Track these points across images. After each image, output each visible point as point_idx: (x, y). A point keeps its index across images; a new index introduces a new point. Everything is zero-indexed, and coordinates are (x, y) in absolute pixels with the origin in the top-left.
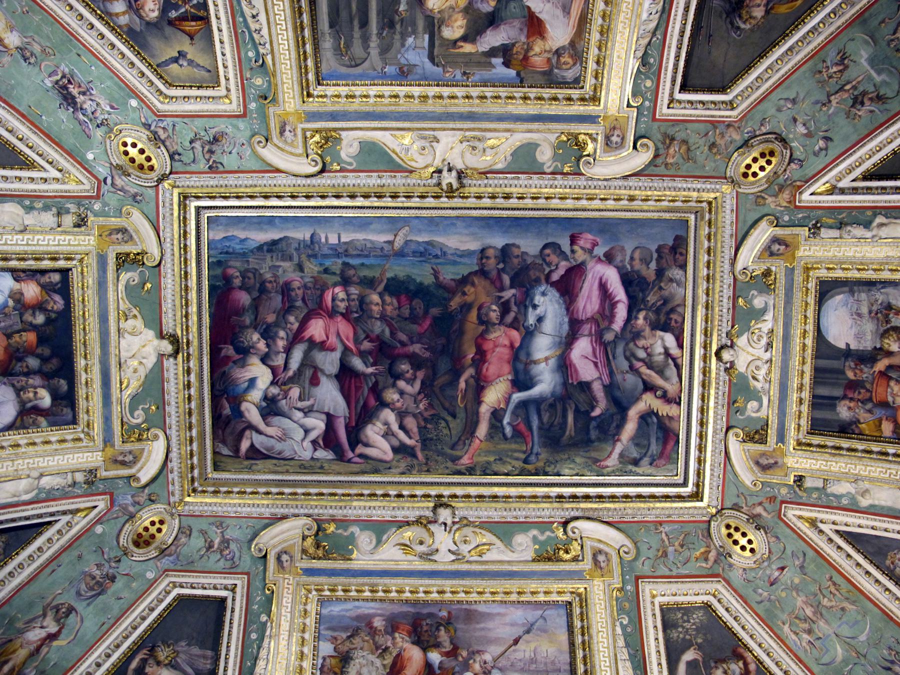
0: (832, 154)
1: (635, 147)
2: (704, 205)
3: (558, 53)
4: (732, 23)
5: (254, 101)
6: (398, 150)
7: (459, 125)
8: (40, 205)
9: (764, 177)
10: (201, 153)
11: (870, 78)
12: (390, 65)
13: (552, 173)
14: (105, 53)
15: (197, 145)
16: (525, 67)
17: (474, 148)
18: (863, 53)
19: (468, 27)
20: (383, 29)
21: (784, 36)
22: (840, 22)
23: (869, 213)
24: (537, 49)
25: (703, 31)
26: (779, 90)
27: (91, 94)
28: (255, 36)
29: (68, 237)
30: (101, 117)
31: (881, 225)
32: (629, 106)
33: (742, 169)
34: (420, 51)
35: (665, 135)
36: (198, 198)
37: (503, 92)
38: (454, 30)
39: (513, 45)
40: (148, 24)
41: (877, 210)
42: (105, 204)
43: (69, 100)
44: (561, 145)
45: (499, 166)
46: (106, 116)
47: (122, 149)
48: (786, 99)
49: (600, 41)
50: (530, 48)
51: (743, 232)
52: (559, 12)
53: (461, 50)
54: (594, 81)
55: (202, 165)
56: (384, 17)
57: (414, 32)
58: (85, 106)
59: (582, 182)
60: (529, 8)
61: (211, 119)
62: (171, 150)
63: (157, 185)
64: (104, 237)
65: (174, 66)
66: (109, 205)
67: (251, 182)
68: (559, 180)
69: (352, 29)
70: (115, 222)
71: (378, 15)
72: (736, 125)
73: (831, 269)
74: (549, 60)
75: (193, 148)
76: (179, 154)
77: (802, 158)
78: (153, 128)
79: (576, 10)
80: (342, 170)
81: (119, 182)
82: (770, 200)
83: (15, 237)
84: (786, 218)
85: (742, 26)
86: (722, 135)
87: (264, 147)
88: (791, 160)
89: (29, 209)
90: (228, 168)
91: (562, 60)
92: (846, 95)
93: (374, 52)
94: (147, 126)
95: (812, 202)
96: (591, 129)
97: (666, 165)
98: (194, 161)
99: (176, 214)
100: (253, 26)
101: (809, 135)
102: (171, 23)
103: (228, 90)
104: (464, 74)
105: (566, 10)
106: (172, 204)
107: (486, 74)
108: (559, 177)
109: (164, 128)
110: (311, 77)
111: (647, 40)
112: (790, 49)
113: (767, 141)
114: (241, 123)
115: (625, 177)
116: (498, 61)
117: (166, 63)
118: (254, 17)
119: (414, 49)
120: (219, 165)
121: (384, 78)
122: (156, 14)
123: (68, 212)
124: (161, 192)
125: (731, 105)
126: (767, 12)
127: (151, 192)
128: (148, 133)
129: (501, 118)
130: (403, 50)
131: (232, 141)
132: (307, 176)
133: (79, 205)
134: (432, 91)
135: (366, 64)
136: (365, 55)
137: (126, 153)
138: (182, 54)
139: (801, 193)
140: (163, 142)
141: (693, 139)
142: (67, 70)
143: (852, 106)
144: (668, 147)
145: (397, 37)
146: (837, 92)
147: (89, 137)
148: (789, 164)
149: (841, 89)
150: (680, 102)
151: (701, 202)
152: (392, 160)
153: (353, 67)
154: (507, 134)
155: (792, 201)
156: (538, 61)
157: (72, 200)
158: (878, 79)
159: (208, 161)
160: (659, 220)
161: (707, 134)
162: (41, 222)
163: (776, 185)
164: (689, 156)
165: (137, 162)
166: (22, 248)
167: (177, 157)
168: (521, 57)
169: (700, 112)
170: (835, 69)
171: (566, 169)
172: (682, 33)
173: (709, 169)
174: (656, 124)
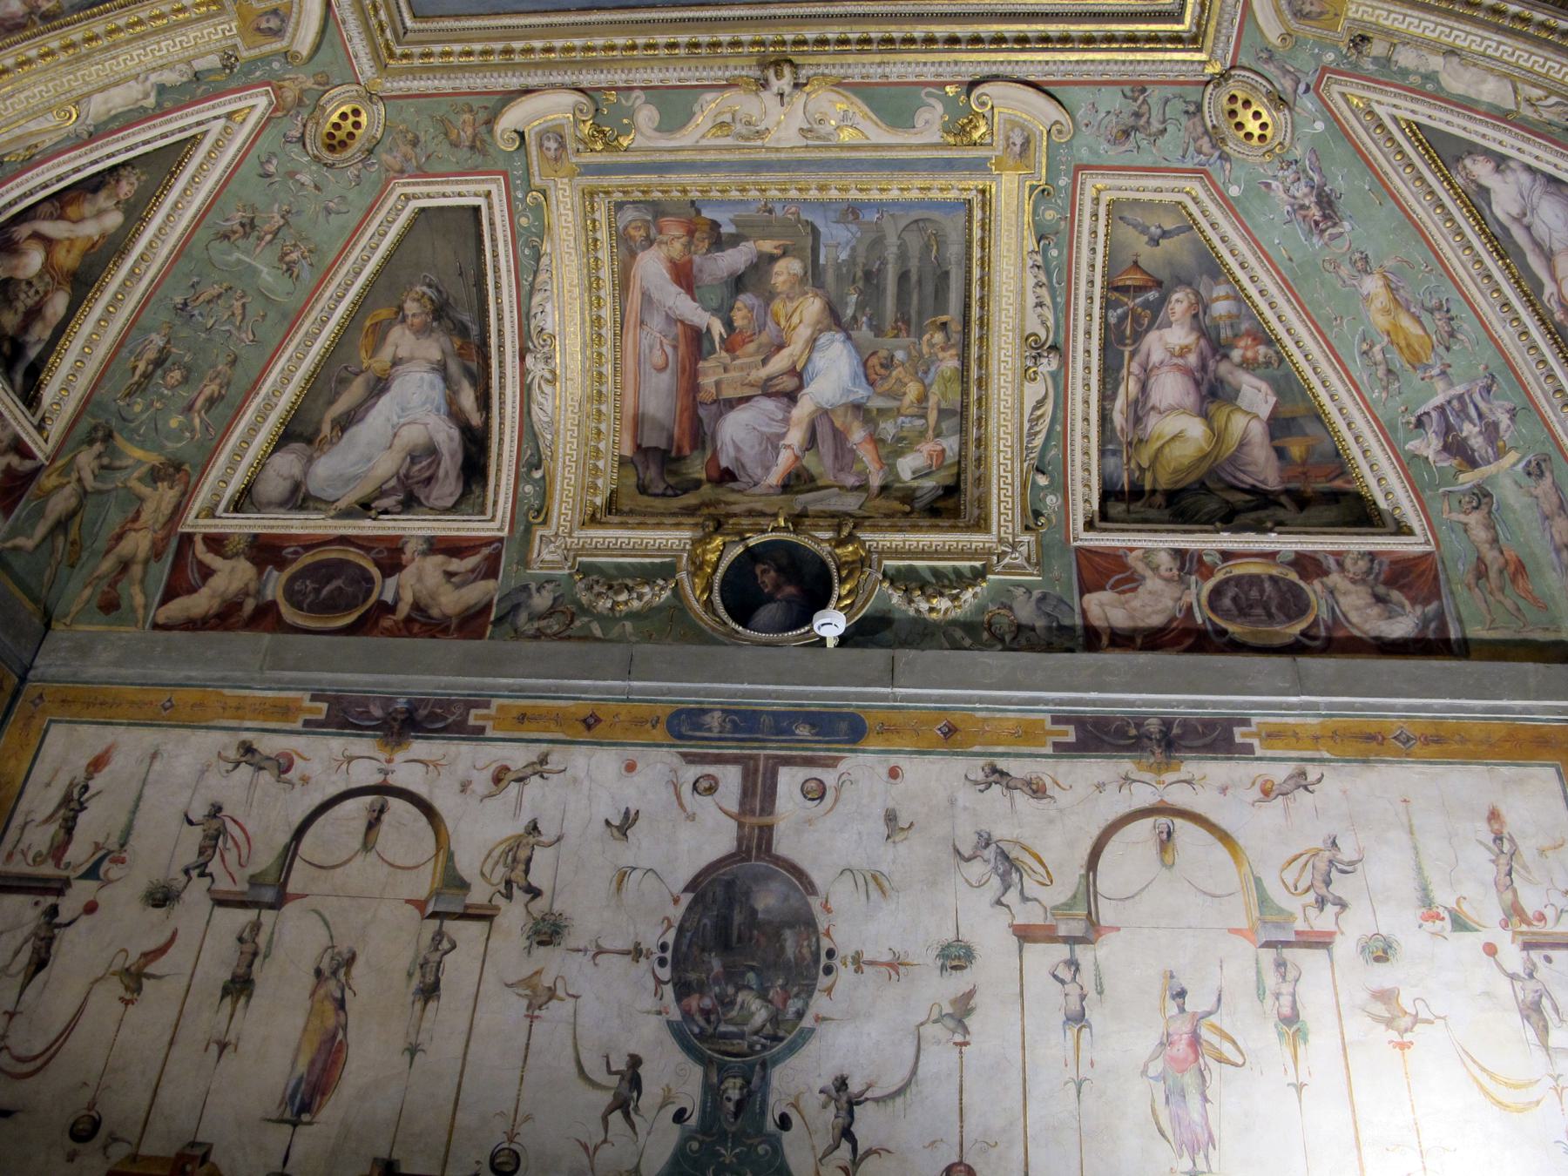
0: (252, 159)
1: (521, 135)
2: (398, 50)
3: (649, 242)
4: (439, 291)
5: (1058, 189)
6: (858, 118)
7: (773, 156)
8: (1412, 78)
9: (330, 115)
10: (1154, 112)
11: (247, 252)
12: (870, 223)
13: (631, 89)
14: (1252, 261)
15: (1156, 126)
16: (691, 221)
17: (749, 123)
18: (270, 279)
19: (768, 273)
20: (879, 270)
21: (371, 285)
22: (314, 314)
23: (168, 105)
24: (678, 246)
25: (472, 281)
26: (354, 225)
27: (1292, 205)
28: (1044, 280)
29: (1388, 23)
30: (1290, 174)
31: (146, 96)
32: (544, 193)
33: (363, 119)
34: (831, 242)
35: (484, 153)
36: (1176, 39)
37: (715, 194)
38: (787, 270)
39: (708, 251)
40: (1189, 284)
41: (160, 111)
42: (1318, 57)
43: (1326, 202)
44: (626, 130)
45: (709, 96)
46: (1280, 174)
47: (1269, 132)
48: (338, 213)
49: (597, 269)
50: (688, 246)
51: (329, 32)
52: (656, 295)
53: (776, 243)
54: (597, 215)
55: (1155, 95)
56: (877, 286)
57: (838, 266)
58: (1306, 190)
59: (587, 79)
60: (694, 299)
61: (1127, 163)
62: (1197, 120)
63: (1232, 67)
64: (1332, 11)
65: (1167, 227)
66: (1312, 55)
67: (1085, 68)
68: (619, 78)
69: (920, 270)
70: (1307, 31)
71: (884, 289)
72: (392, 174)
73: (179, 11)
74: (660, 232)
75: (1164, 121)
76: (1187, 112)
77: (289, 146)
78: (1217, 154)
79: (635, 298)
80: (944, 85)
81: (1288, 84)
82: (309, 84)
83: (1465, 44)
84: (276, 65)
85: (425, 289)
86: (407, 159)
87: (1057, 122)
88: (302, 140)
89: (1431, 77)
90: (1117, 89)
91: (642, 233)
92: (266, 227)
93: (892, 240)
94: (1224, 157)
95: (251, 96)
96: (588, 158)
97: (471, 111)
98: (1167, 101)
99: (1213, 23)
100: (1044, 292)
101: (291, 174)
102: (1159, 284)
103: (1096, 201)
104: (770, 211)
105: (647, 298)
106: (1216, 38)
107: (742, 212)
108: (621, 84)
109: (1199, 152)
110: (977, 214)
111: (540, 278)
112: (358, 274)
113: (343, 161)
114: (1084, 155)
115: (527, 91)
116: (727, 229)
117: (1179, 231)
118: (1040, 305)
119: (838, 243)
120: (1129, 94)
121: (879, 206)
122: (1175, 297)
123: (1375, 58)
124: (1229, 57)
125: (408, 198)
126: (401, 308)
127: (1243, 60)
128: (1226, 149)
129: (714, 166)
130: (854, 242)
131: (1102, 129)
132: (995, 78)
133: (1356, 66)
134: (813, 194)
135: (903, 223)
136: (906, 236)
137: (1264, 126)
138: (1155, 242)
139: (270, 103)
140: (1206, 132)
141: (444, 150)
142: (1315, 239)
143: (252, 219)
144: (475, 136)
145: (861, 260)
146: (279, 229)
147: (1313, 151)
148: (303, 135)
149: (276, 234)
150: (476, 195)
151: (405, 56)
152: (869, 101)
153: (923, 220)
154: (704, 142)
155: (278, 90)
156: (674, 230)
157: (1364, 73)
158: (237, 255)
159: (1145, 101)
160: (457, 16)
161: (428, 157)
162: (1421, 57)
163: (307, 103)
164: (444, 126)
165: (1250, 113)
166: (1462, 27)
167: (1192, 108)
168: (697, 235)
169: (448, 189)
170: (294, 256)
171: (613, 97)
172: (497, 287)
173: (410, 109)
174: (501, 166)
